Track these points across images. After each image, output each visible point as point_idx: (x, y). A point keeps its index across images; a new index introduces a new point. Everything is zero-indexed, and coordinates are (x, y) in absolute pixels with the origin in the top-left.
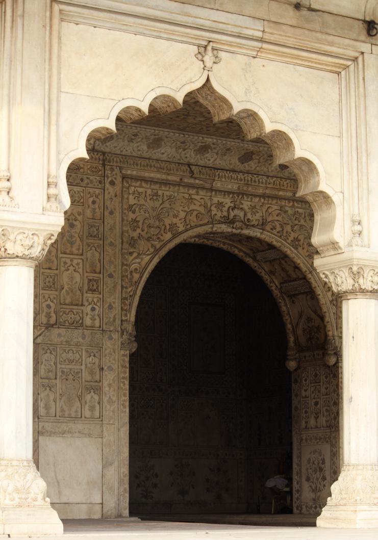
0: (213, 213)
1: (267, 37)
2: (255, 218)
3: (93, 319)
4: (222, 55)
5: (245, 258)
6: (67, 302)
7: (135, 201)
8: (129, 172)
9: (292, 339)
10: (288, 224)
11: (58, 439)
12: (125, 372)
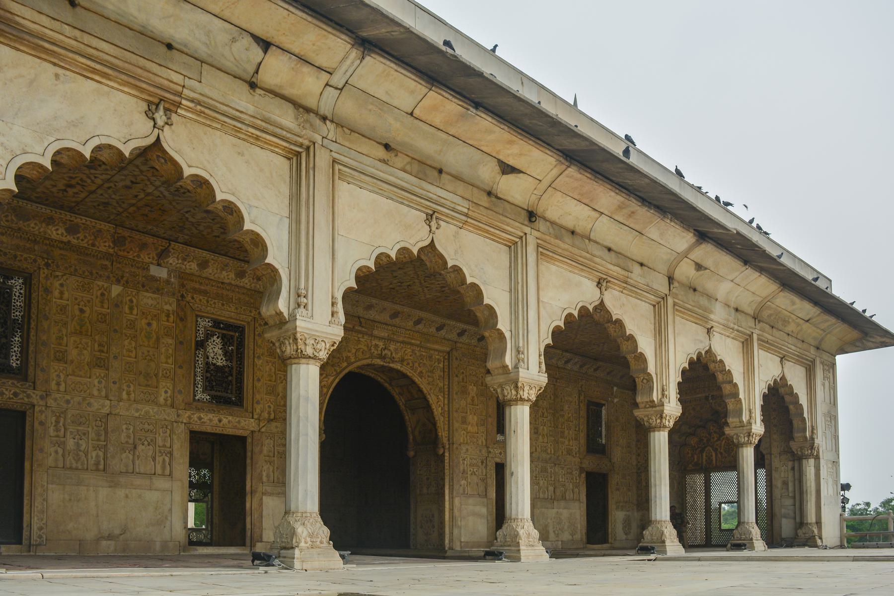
1: (470, 213)
2: (397, 356)
4: (442, 223)
9: (411, 437)
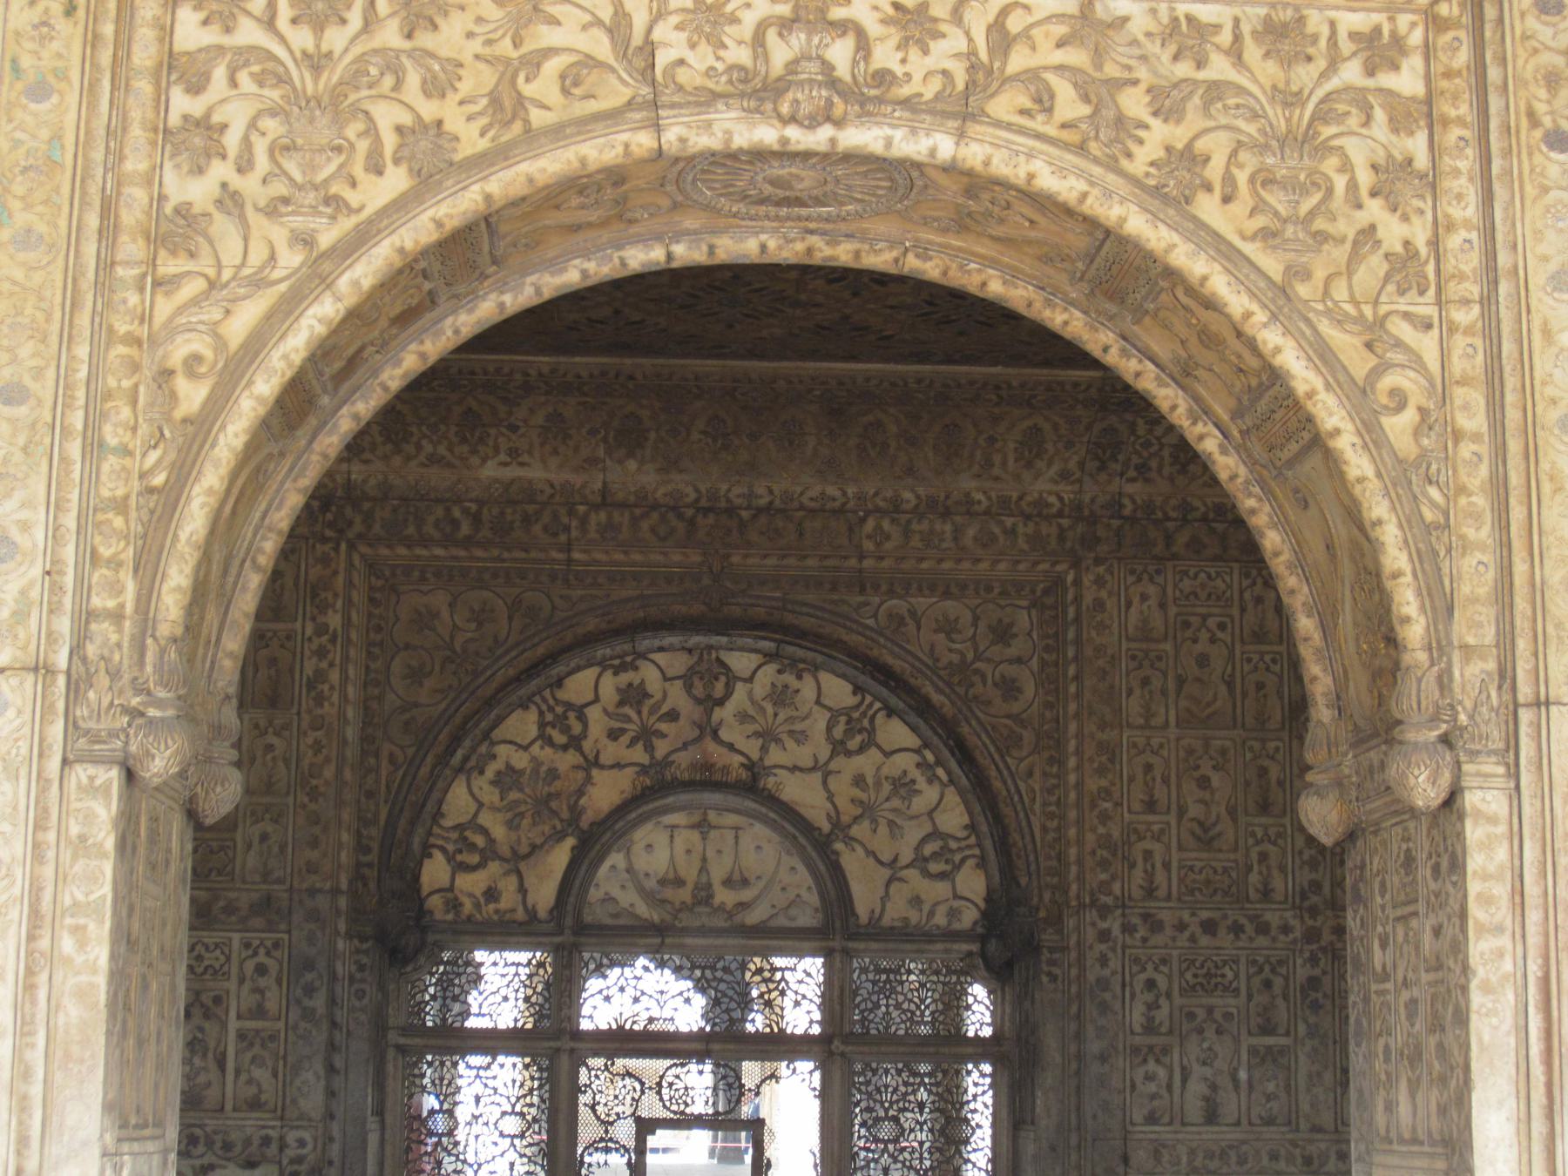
0: (663, 59)
5: (1047, 313)
10: (1135, 82)
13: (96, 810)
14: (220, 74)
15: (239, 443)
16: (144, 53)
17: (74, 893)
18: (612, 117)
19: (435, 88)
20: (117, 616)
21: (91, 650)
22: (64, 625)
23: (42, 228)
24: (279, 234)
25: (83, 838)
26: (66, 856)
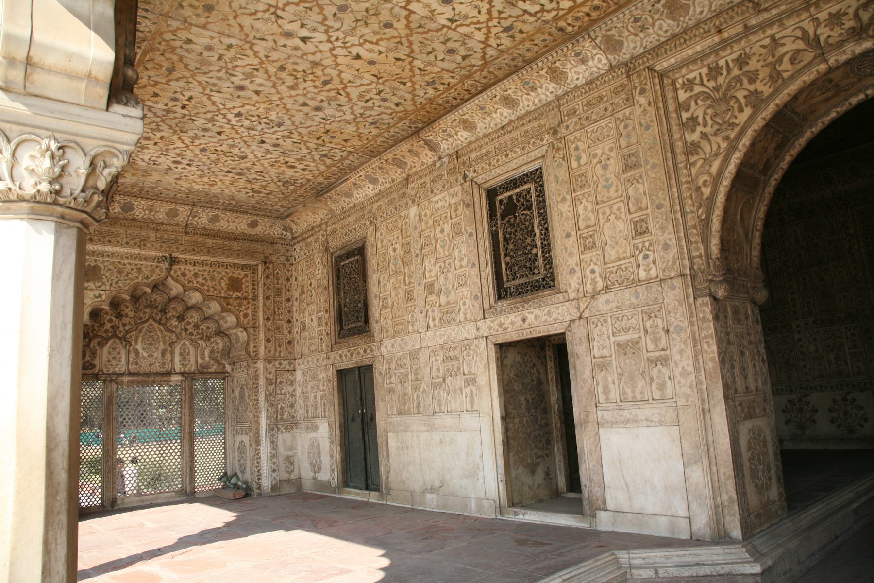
3: (647, 270)
6: (613, 258)
7: (688, 95)
8: (665, 64)
11: (622, 430)
12: (708, 328)
13: (706, 309)
14: (693, 103)
15: (723, 200)
16: (672, 107)
17: (704, 333)
18: (810, 64)
19: (752, 81)
20: (700, 256)
21: (695, 267)
22: (686, 262)
23: (657, 162)
24: (719, 140)
25: (704, 318)
26: (700, 323)
